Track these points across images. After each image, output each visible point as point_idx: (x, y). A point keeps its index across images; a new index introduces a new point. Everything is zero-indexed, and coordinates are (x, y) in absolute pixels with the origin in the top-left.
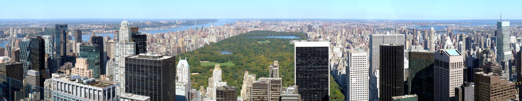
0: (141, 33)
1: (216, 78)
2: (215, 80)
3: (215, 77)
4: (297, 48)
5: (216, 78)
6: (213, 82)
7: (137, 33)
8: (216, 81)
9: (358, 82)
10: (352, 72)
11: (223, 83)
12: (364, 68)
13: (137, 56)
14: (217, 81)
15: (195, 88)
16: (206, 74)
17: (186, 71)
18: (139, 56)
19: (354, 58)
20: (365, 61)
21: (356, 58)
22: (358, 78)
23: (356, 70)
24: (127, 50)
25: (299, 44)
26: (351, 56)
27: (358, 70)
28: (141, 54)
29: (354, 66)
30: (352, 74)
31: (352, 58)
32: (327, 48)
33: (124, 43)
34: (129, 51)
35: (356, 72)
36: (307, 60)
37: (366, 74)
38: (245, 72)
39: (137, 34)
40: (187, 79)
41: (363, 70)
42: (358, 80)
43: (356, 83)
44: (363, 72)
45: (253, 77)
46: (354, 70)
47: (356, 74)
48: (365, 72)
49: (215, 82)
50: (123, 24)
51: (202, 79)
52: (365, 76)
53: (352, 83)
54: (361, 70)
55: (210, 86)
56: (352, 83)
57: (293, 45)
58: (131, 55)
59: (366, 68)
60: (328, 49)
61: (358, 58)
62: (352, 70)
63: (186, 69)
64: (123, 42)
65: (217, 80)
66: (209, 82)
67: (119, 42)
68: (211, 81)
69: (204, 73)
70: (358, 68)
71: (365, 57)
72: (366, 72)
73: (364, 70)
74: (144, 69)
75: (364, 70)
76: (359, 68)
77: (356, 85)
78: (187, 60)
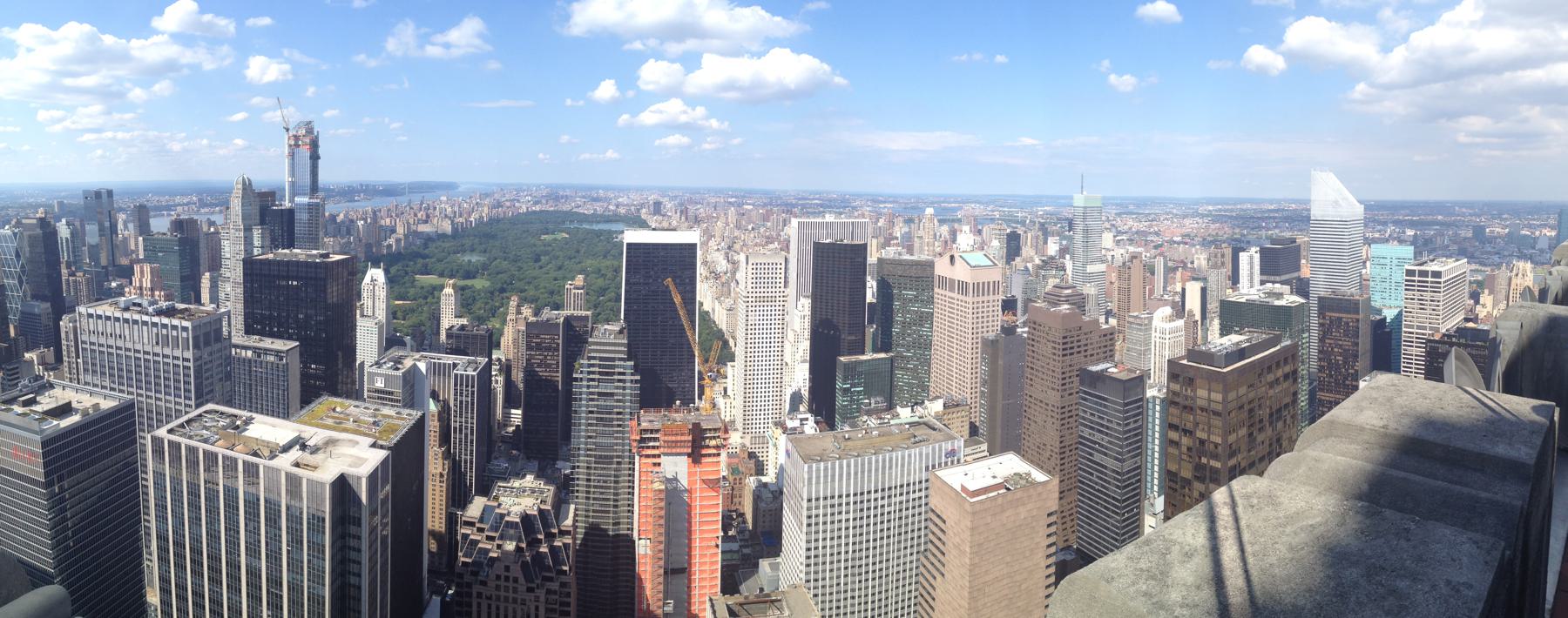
9: (761, 322)
10: (750, 299)
12: (778, 290)
19: (754, 267)
21: (759, 266)
22: (761, 313)
23: (758, 295)
26: (747, 263)
27: (762, 295)
29: (754, 285)
31: (750, 267)
37: (782, 303)
41: (774, 294)
42: (761, 318)
43: (757, 322)
46: (754, 295)
47: (758, 304)
56: (750, 323)
62: (750, 295)
70: (762, 290)
71: (779, 266)
72: (782, 299)
73: (778, 294)
75: (778, 294)
76: (766, 290)
77: (757, 327)
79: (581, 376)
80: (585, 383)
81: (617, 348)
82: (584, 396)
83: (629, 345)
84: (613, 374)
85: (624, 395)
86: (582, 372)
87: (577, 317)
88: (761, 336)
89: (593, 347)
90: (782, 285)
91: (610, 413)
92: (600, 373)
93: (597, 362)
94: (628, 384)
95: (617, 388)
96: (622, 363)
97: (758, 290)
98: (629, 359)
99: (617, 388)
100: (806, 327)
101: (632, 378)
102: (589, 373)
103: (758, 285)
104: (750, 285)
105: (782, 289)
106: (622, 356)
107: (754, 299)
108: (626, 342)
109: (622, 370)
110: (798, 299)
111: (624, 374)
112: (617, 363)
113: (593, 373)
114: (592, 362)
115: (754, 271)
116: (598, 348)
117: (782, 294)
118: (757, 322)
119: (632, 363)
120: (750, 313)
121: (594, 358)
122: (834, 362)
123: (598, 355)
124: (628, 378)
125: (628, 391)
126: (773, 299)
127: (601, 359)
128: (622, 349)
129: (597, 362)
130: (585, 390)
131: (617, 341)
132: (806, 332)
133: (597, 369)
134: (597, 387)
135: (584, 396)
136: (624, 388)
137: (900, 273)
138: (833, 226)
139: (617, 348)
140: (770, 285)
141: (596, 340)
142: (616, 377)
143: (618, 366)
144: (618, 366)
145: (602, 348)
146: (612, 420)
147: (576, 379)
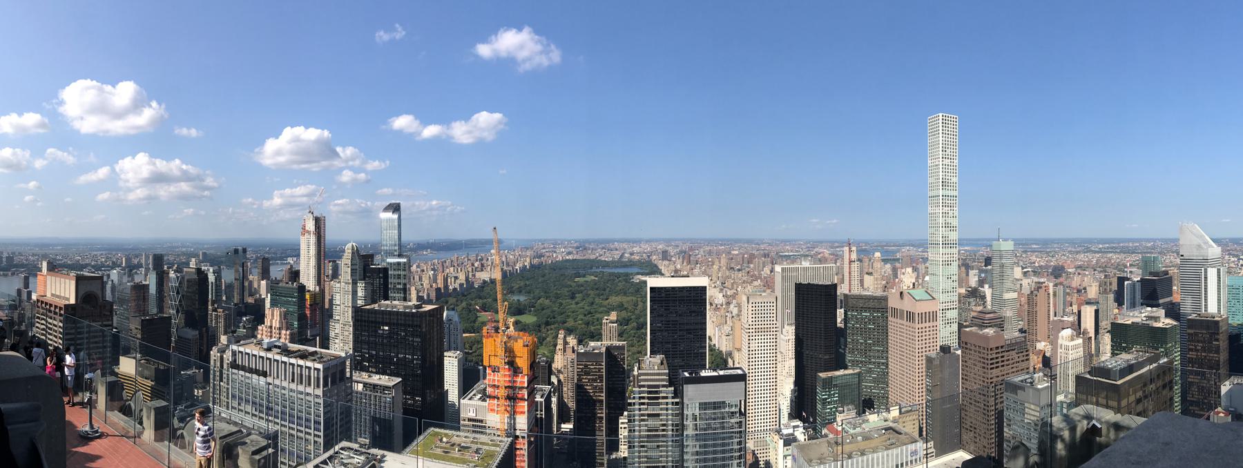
4: (651, 288)
9: (760, 348)
10: (751, 331)
19: (754, 305)
20: (772, 312)
21: (757, 305)
22: (760, 341)
23: (757, 327)
25: (653, 282)
26: (748, 303)
27: (760, 326)
29: (754, 320)
30: (751, 334)
31: (750, 305)
32: (702, 290)
35: (757, 330)
36: (669, 309)
37: (774, 333)
38: (560, 332)
41: (769, 326)
42: (760, 345)
43: (757, 349)
44: (769, 330)
45: (572, 341)
46: (754, 327)
47: (757, 334)
48: (772, 330)
52: (771, 337)
53: (751, 349)
54: (766, 326)
56: (751, 349)
57: (645, 282)
59: (775, 322)
60: (706, 290)
61: (760, 305)
62: (751, 327)
71: (772, 304)
72: (774, 329)
76: (763, 323)
77: (757, 352)
79: (634, 401)
80: (637, 407)
81: (661, 377)
82: (637, 418)
83: (669, 375)
84: (658, 398)
85: (667, 415)
86: (634, 398)
87: (619, 346)
88: (760, 359)
89: (642, 377)
90: (774, 319)
91: (657, 431)
92: (649, 398)
93: (646, 389)
94: (670, 406)
95: (661, 409)
96: (665, 389)
97: (757, 323)
98: (670, 386)
99: (661, 409)
100: (790, 348)
101: (673, 400)
102: (640, 398)
103: (757, 319)
104: (750, 320)
105: (775, 322)
106: (665, 383)
107: (753, 331)
108: (667, 371)
109: (665, 395)
110: (783, 327)
111: (666, 398)
112: (661, 389)
113: (643, 398)
114: (642, 389)
115: (754, 309)
116: (646, 377)
117: (774, 326)
118: (757, 349)
119: (673, 389)
120: (751, 342)
121: (643, 386)
122: (815, 377)
123: (646, 383)
124: (670, 400)
125: (670, 412)
126: (768, 330)
127: (649, 386)
128: (665, 377)
129: (646, 389)
130: (637, 412)
131: (661, 371)
132: (790, 352)
133: (646, 395)
134: (647, 409)
135: (637, 418)
136: (667, 409)
137: (861, 305)
138: (809, 271)
139: (661, 377)
140: (766, 319)
141: (644, 372)
142: (660, 401)
143: (661, 392)
144: (661, 392)
145: (649, 377)
146: (658, 436)
147: (630, 404)
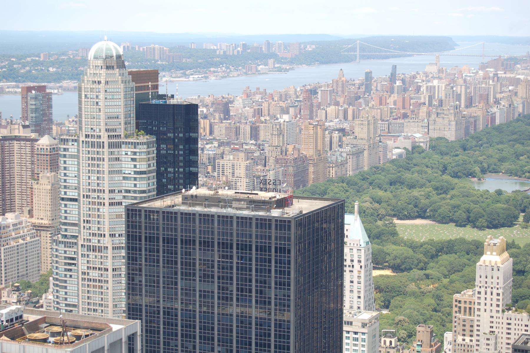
0: (173, 96)
1: (489, 296)
2: (482, 301)
3: (483, 290)
5: (489, 296)
6: (477, 313)
7: (153, 98)
8: (488, 307)
11: (519, 316)
13: (178, 199)
14: (495, 308)
15: (393, 335)
16: (427, 276)
17: (356, 259)
18: (185, 198)
24: (120, 172)
28: (193, 191)
33: (105, 139)
34: (125, 178)
39: (154, 102)
40: (362, 295)
49: (482, 312)
50: (96, 58)
51: (414, 294)
55: (459, 329)
58: (135, 192)
63: (355, 251)
64: (99, 137)
65: (495, 303)
66: (455, 309)
67: (83, 138)
68: (462, 305)
69: (416, 273)
74: (212, 256)
78: (360, 213)
